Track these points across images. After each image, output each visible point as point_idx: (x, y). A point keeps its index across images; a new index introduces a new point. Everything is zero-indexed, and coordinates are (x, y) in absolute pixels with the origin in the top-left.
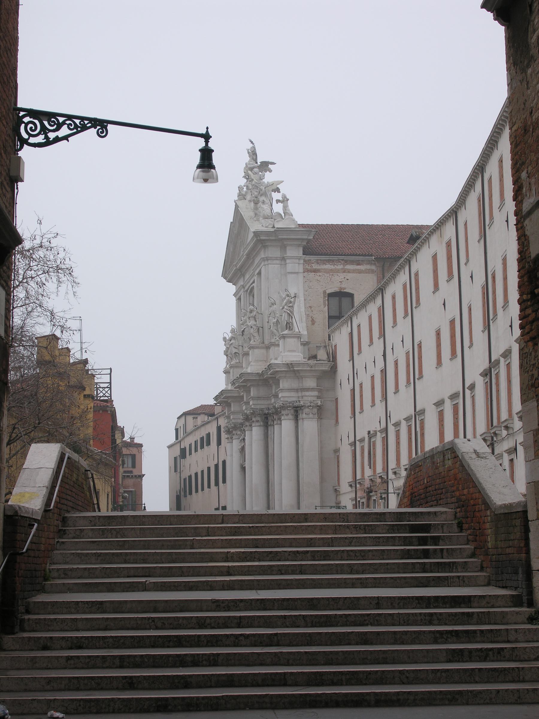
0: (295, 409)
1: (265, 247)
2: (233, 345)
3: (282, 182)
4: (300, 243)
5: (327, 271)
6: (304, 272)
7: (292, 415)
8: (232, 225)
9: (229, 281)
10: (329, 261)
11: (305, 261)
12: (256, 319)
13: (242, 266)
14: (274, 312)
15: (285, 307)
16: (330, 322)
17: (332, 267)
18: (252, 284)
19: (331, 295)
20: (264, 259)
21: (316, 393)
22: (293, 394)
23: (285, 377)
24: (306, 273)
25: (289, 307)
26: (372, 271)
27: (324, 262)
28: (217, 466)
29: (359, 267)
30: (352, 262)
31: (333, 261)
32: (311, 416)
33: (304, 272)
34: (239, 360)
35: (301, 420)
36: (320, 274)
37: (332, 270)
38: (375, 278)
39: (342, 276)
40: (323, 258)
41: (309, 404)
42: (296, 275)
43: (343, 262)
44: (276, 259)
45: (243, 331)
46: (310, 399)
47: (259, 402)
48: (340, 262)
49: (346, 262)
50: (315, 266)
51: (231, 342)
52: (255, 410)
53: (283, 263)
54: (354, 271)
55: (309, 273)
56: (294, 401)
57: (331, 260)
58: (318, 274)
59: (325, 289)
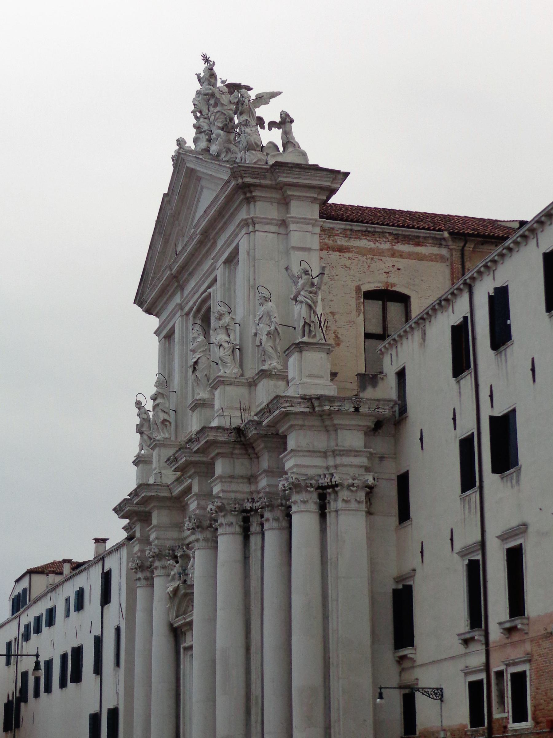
0: (321, 491)
1: (249, 200)
2: (160, 407)
3: (279, 93)
4: (315, 195)
5: (362, 252)
6: (321, 250)
7: (315, 503)
8: (166, 199)
9: (149, 311)
10: (366, 233)
11: (323, 229)
12: (230, 331)
13: (183, 268)
14: (268, 314)
15: (302, 293)
16: (367, 344)
17: (371, 245)
18: (209, 287)
19: (370, 295)
20: (246, 223)
21: (363, 461)
22: (318, 461)
23: (302, 426)
24: (325, 252)
25: (310, 292)
26: (442, 258)
27: (356, 234)
28: (99, 642)
29: (419, 249)
30: (407, 239)
31: (374, 233)
32: (354, 505)
33: (321, 250)
34: (170, 434)
35: (333, 514)
36: (350, 255)
37: (371, 251)
38: (447, 271)
39: (389, 261)
40: (357, 227)
41: (350, 481)
42: (306, 253)
43: (390, 238)
44: (270, 222)
45: (196, 363)
46: (353, 471)
47: (234, 487)
48: (386, 237)
49: (397, 238)
50: (341, 241)
51: (157, 402)
52: (225, 502)
53: (282, 230)
54: (410, 256)
55: (331, 252)
56: (320, 476)
57: (369, 232)
58: (347, 255)
59: (360, 283)
